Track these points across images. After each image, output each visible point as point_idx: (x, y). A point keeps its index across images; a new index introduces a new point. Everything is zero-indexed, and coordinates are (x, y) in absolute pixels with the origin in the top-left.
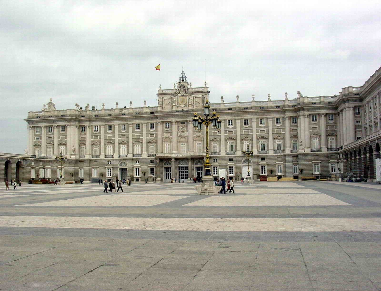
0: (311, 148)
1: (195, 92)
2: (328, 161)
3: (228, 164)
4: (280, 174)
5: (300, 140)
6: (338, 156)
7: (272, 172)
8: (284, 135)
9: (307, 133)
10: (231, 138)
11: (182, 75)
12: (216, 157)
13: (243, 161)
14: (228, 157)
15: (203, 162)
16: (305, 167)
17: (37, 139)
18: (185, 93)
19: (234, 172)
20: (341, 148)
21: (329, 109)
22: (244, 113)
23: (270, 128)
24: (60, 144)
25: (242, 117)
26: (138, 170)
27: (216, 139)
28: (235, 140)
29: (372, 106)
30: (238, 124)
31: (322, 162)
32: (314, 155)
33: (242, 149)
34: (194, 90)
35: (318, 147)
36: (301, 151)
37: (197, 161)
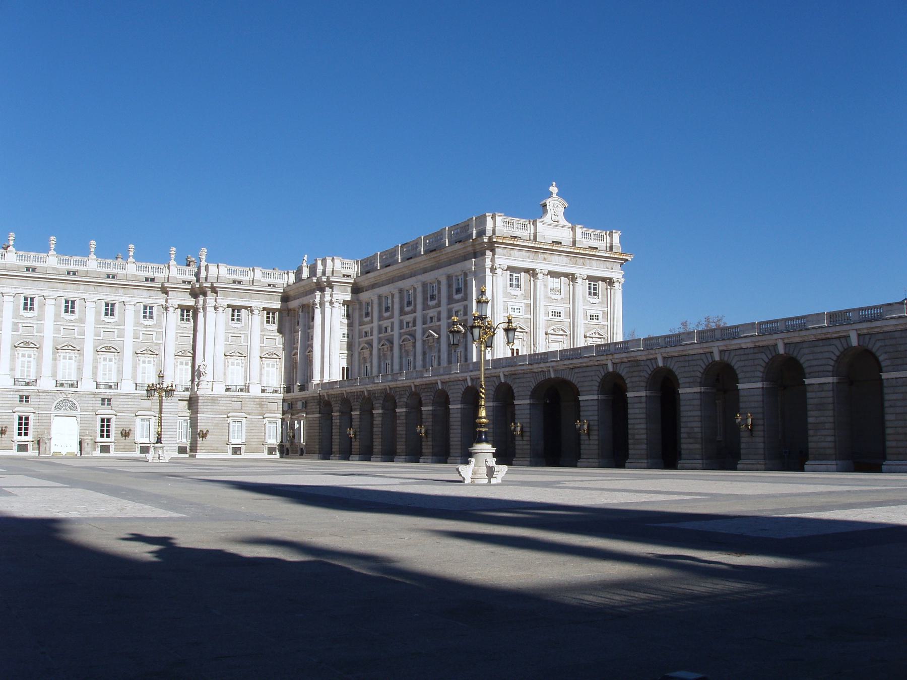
0: (225, 382)
2: (263, 414)
3: (16, 409)
4: (147, 441)
5: (204, 363)
7: (126, 434)
8: (160, 349)
9: (221, 350)
10: (27, 345)
13: (56, 403)
14: (18, 390)
16: (212, 427)
19: (30, 432)
21: (271, 300)
23: (129, 328)
25: (61, 294)
28: (38, 348)
29: (397, 307)
30: (50, 309)
31: (248, 417)
32: (233, 399)
33: (54, 374)
35: (241, 383)
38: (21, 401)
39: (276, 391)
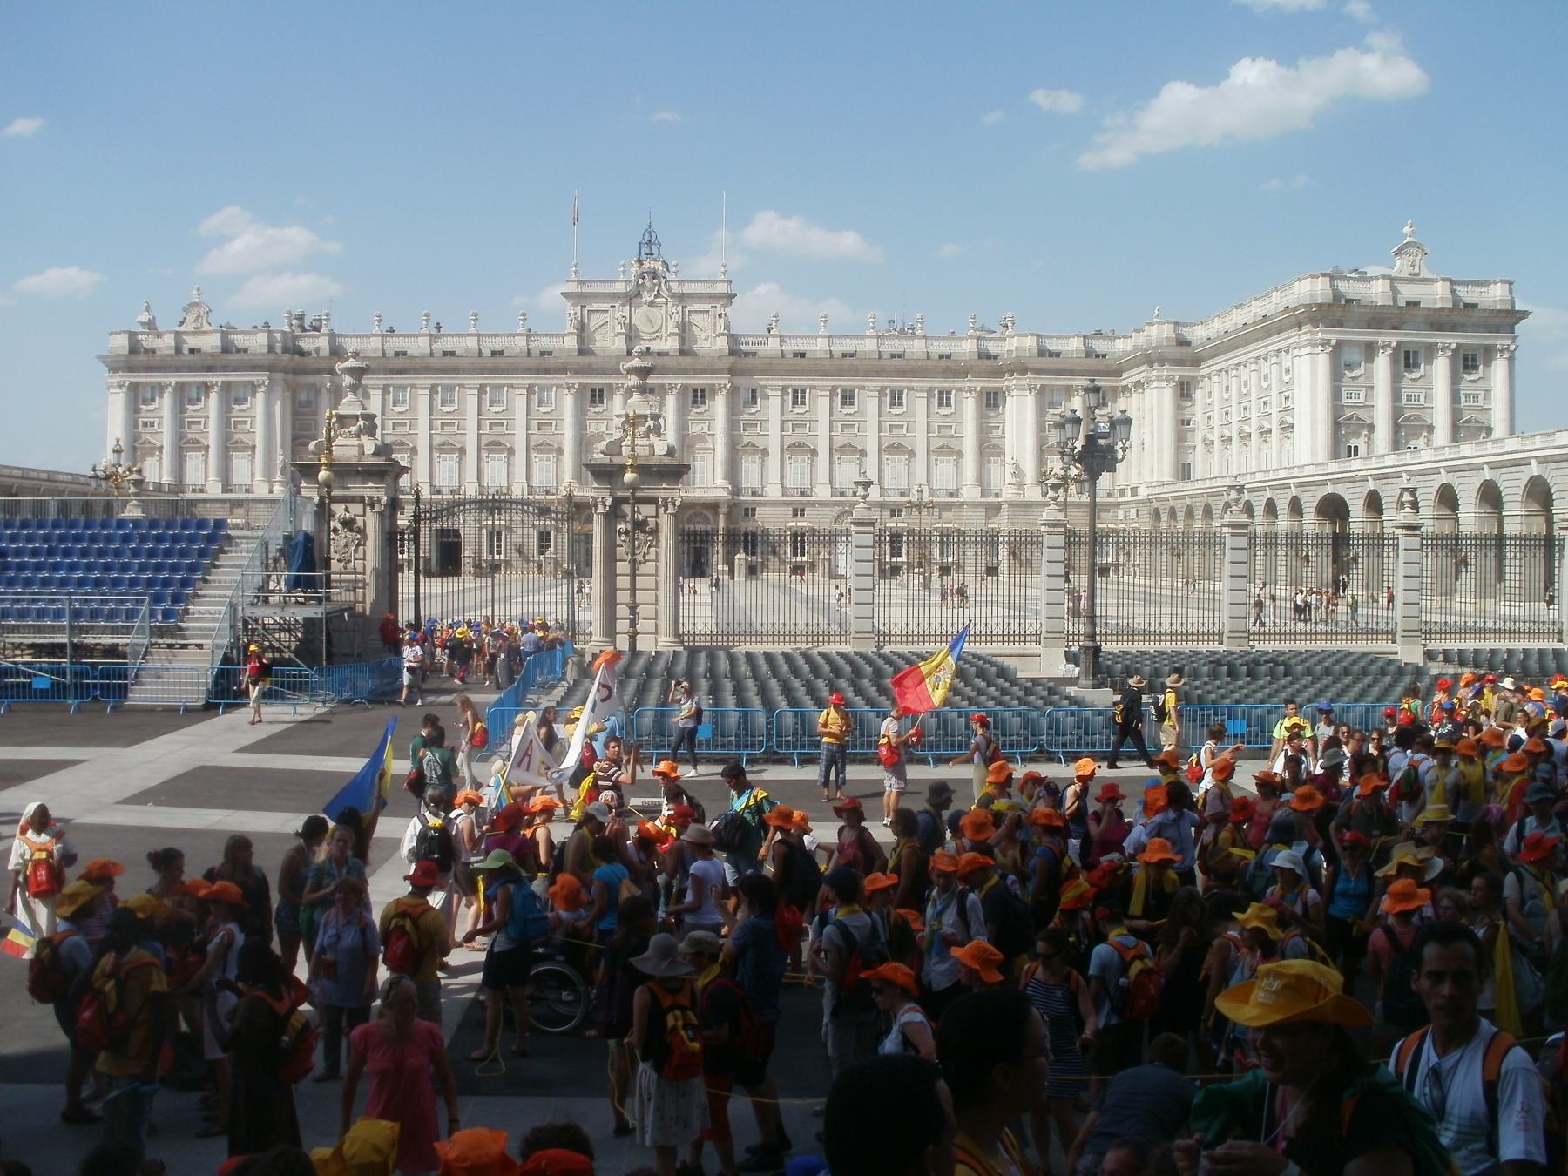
1: (692, 296)
6: (1121, 513)
11: (647, 235)
12: (754, 502)
15: (711, 517)
17: (145, 425)
18: (656, 296)
20: (1134, 491)
22: (840, 372)
24: (229, 446)
26: (494, 534)
27: (753, 445)
34: (688, 289)
36: (1008, 494)
37: (691, 512)
38: (795, 514)
39: (1109, 495)
